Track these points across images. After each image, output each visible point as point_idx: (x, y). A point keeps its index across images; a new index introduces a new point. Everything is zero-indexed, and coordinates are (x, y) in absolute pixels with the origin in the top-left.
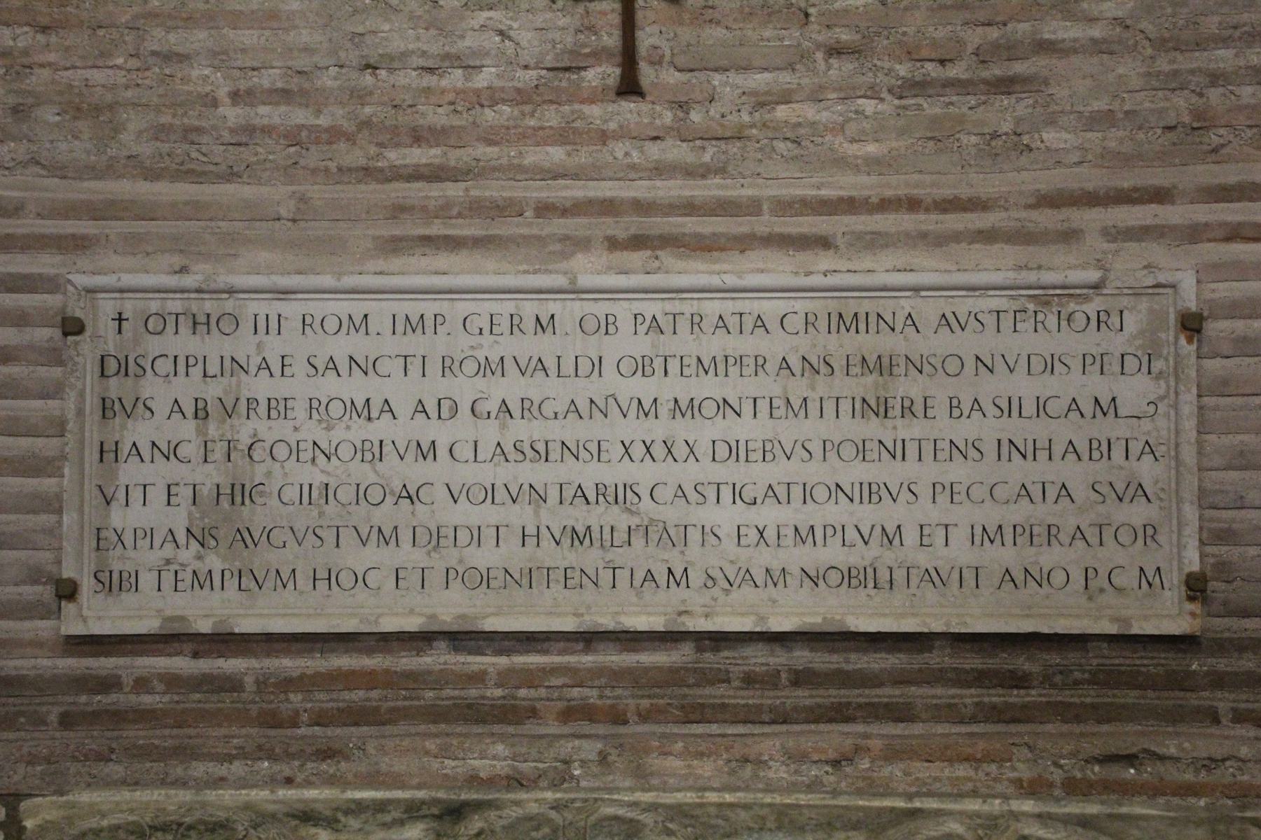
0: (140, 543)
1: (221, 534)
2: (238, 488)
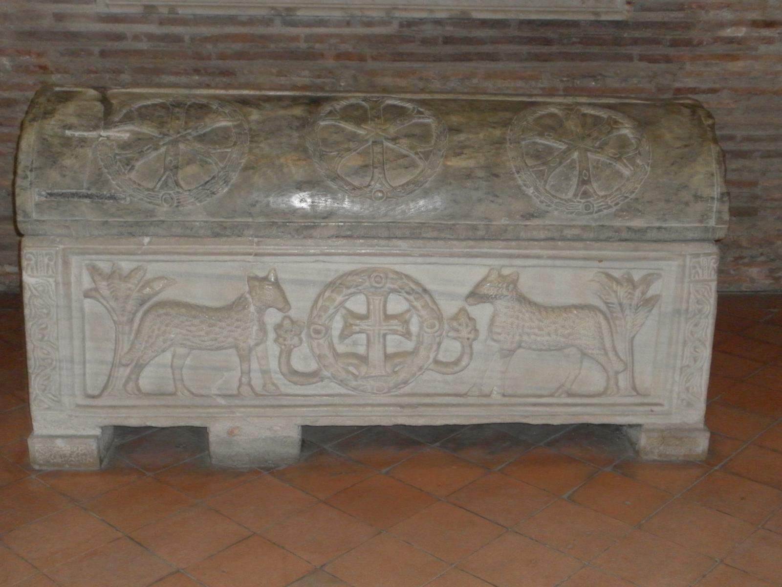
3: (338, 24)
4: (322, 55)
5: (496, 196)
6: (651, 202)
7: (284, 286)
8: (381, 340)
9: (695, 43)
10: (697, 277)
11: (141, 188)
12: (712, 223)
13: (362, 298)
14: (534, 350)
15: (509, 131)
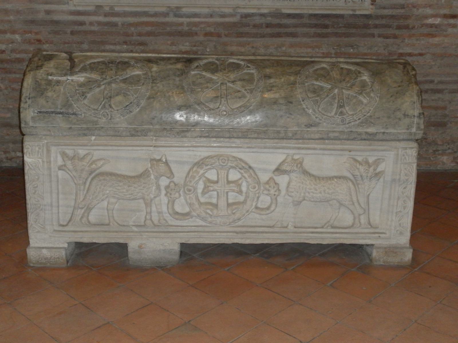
3: (206, 16)
4: (196, 34)
5: (291, 114)
6: (379, 118)
7: (170, 164)
8: (225, 195)
9: (410, 27)
10: (405, 161)
11: (90, 109)
12: (414, 130)
13: (214, 171)
14: (312, 201)
15: (298, 78)
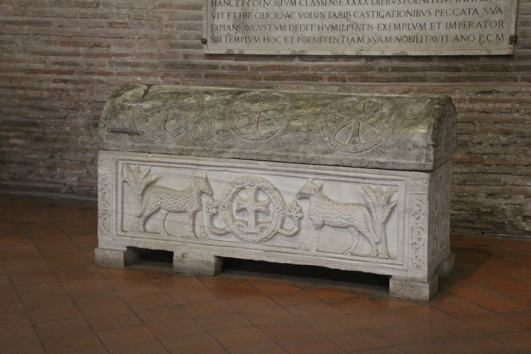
0: (221, 29)
1: (241, 27)
2: (245, 13)
11: (149, 129)
12: (423, 161)
